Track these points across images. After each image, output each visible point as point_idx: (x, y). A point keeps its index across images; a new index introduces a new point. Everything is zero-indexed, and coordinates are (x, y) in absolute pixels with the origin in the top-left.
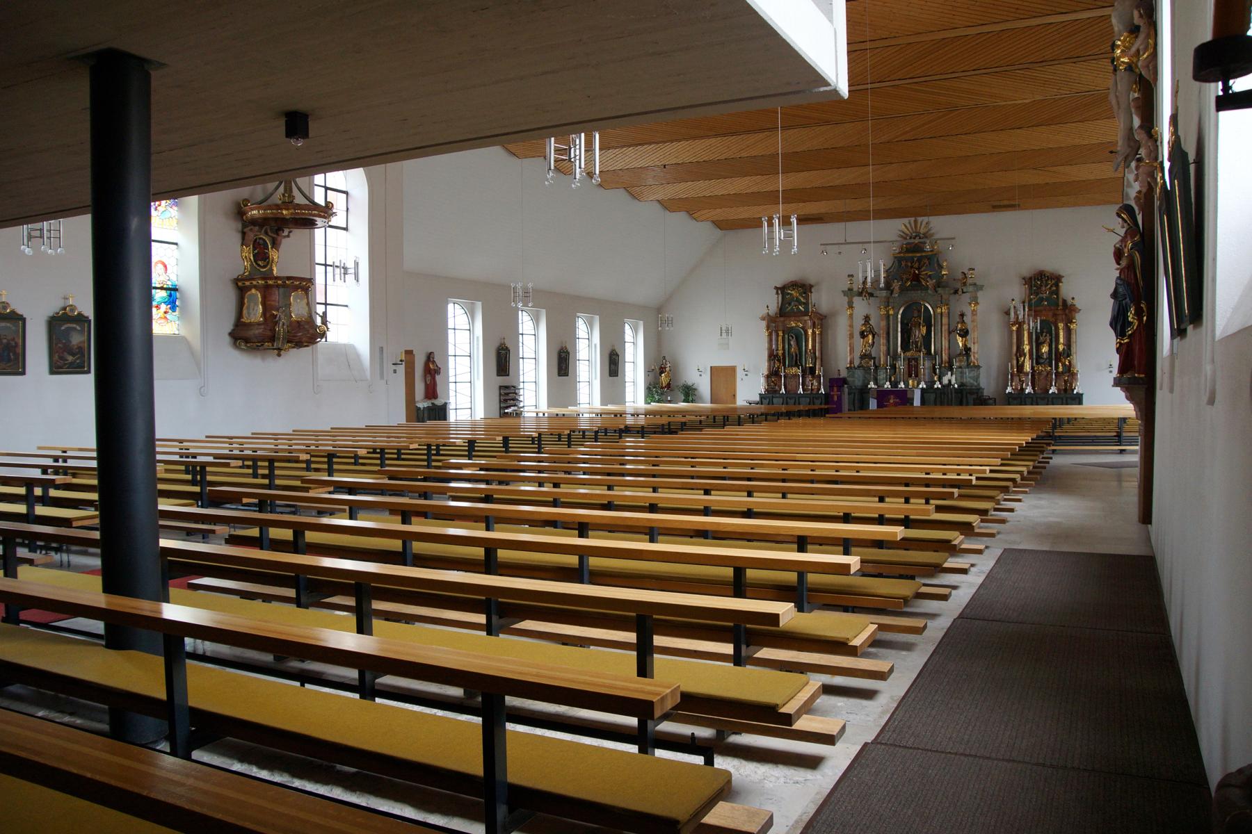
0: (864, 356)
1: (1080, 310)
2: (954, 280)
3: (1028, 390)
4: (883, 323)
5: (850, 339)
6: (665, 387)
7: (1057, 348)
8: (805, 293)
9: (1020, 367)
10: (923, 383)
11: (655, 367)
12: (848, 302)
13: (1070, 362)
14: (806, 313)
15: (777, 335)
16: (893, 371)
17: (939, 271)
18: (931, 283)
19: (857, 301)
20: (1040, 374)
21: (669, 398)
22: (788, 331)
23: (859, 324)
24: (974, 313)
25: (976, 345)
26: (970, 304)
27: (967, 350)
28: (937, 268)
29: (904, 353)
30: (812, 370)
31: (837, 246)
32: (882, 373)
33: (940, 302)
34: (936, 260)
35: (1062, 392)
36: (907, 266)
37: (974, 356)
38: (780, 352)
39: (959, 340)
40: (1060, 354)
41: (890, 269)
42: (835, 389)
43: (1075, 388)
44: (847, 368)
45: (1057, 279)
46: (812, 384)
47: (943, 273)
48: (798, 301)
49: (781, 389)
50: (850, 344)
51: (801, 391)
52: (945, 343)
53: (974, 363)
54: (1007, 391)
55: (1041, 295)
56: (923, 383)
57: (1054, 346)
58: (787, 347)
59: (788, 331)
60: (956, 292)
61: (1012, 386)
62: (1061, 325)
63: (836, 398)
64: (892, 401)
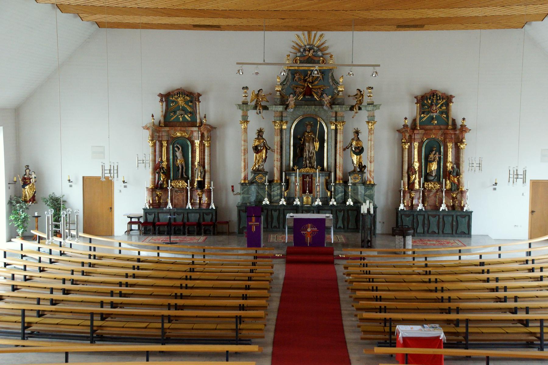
0: (256, 172)
1: (470, 130)
2: (349, 96)
3: (420, 207)
4: (277, 139)
5: (245, 154)
6: (30, 201)
7: (445, 167)
8: (191, 102)
9: (411, 185)
10: (318, 200)
11: (17, 178)
12: (243, 116)
13: (458, 180)
14: (193, 124)
15: (161, 146)
17: (334, 87)
18: (327, 99)
19: (252, 114)
20: (430, 191)
21: (36, 214)
22: (173, 141)
23: (252, 141)
24: (372, 132)
25: (372, 164)
26: (368, 122)
27: (362, 168)
28: (331, 84)
30: (201, 184)
31: (256, 66)
32: (276, 188)
34: (330, 75)
35: (450, 209)
37: (370, 175)
38: (165, 164)
39: (355, 158)
40: (450, 173)
42: (254, 219)
43: (464, 206)
44: (242, 184)
45: (448, 99)
46: (200, 199)
47: (340, 89)
48: (184, 109)
49: (166, 204)
50: (245, 159)
51: (189, 206)
52: (340, 160)
53: (370, 181)
54: (400, 208)
55: (432, 114)
56: (318, 200)
57: (442, 164)
58: (171, 157)
59: (173, 141)
60: (352, 108)
61: (404, 203)
62: (450, 145)
63: (254, 229)
64: (309, 230)
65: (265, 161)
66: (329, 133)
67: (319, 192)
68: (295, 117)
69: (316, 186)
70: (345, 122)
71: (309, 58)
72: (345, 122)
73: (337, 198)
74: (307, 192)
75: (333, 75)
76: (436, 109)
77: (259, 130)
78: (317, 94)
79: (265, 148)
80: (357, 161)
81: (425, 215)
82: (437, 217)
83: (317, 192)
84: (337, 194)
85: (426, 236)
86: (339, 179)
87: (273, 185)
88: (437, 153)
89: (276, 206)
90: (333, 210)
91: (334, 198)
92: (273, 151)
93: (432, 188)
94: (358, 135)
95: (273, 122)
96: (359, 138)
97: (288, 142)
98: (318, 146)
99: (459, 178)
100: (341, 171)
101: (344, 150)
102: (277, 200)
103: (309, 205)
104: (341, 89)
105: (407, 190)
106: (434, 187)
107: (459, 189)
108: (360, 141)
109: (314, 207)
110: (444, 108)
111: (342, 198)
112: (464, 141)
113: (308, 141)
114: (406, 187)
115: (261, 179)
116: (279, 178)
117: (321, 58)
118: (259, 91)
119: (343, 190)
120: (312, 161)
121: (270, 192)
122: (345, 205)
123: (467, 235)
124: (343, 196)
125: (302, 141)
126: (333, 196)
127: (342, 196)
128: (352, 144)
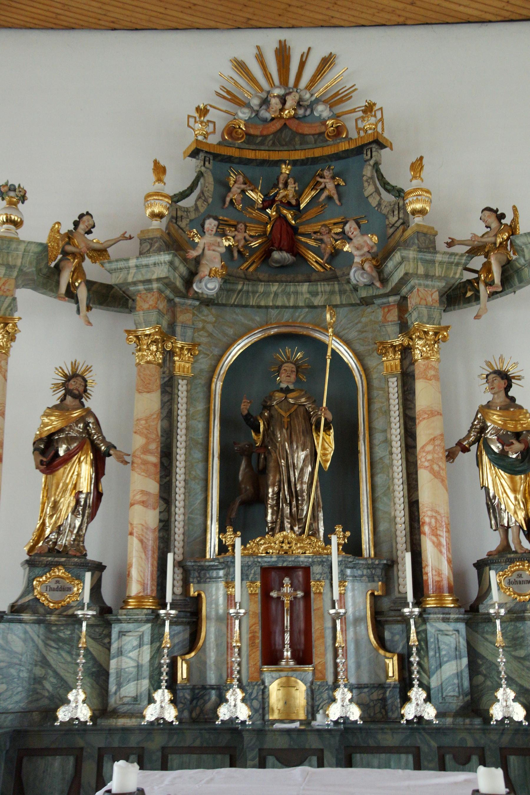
16: (184, 634)
29: (244, 543)
32: (130, 641)
33: (392, 329)
36: (250, 203)
41: (184, 195)
65: (92, 516)
66: (375, 393)
67: (345, 656)
68: (231, 332)
69: (329, 624)
70: (446, 328)
71: (281, 130)
72: (446, 328)
73: (434, 683)
74: (287, 654)
75: (378, 171)
77: (68, 371)
78: (317, 251)
79: (87, 447)
80: (516, 499)
83: (336, 656)
84: (433, 663)
86: (439, 590)
87: (119, 621)
89: (125, 730)
90: (424, 749)
91: (421, 685)
92: (127, 459)
94: (509, 387)
95: (129, 332)
96: (513, 399)
97: (200, 437)
98: (331, 451)
100: (444, 550)
101: (451, 455)
102: (136, 699)
103: (297, 725)
104: (418, 206)
108: (521, 408)
109: (320, 732)
111: (460, 686)
113: (286, 420)
115: (58, 594)
116: (151, 589)
117: (329, 122)
118: (76, 224)
119: (463, 643)
120: (307, 510)
121: (101, 659)
122: (478, 721)
124: (466, 674)
125: (257, 431)
126: (415, 675)
127: (459, 675)
128: (483, 429)
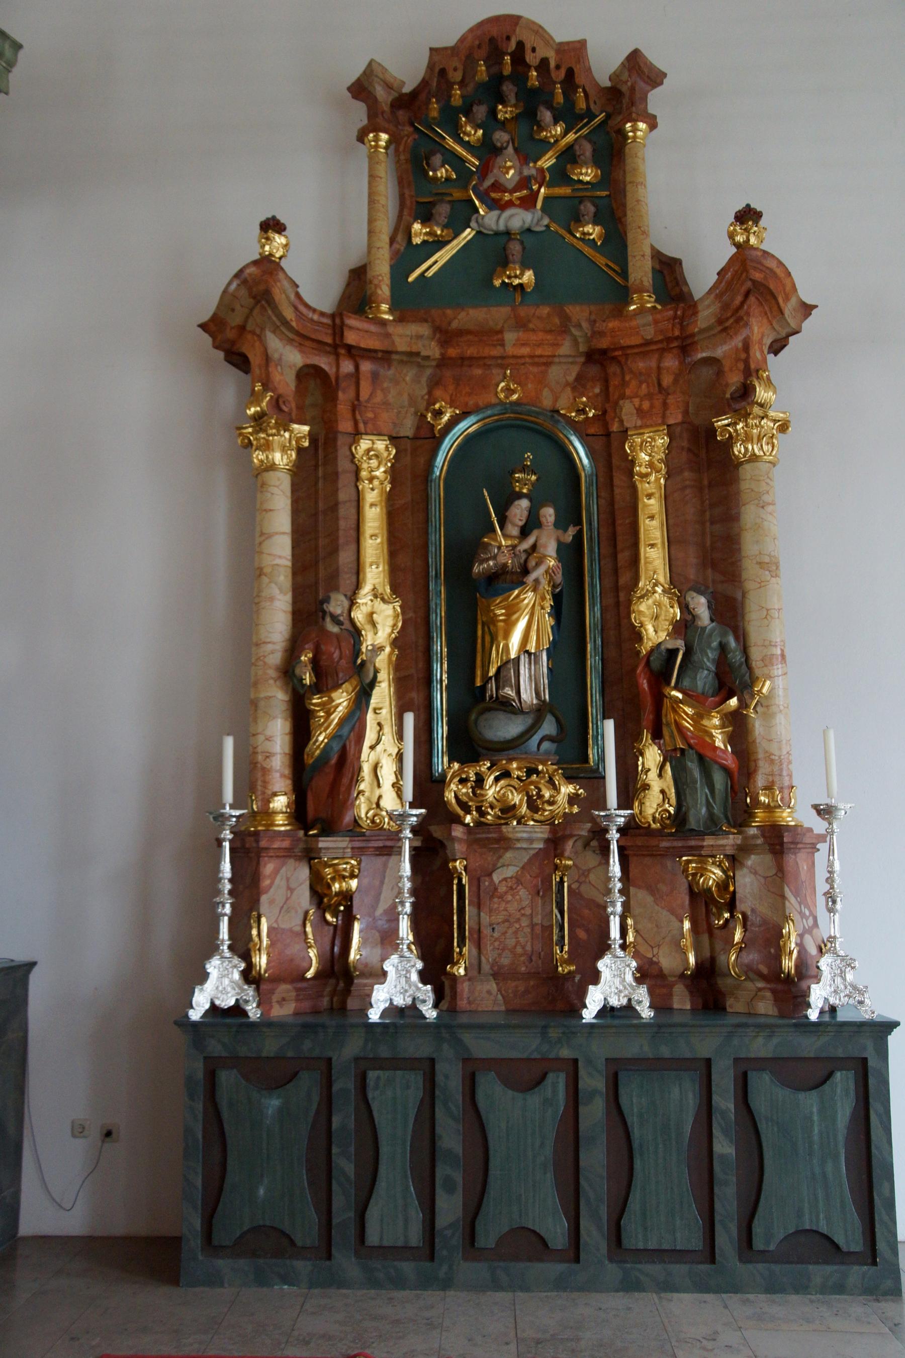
35: (681, 1000)
57: (592, 615)
76: (524, 182)
81: (441, 1068)
82: (557, 1083)
85: (446, 1284)
88: (548, 514)
93: (508, 810)
99: (743, 704)
105: (281, 823)
106: (533, 806)
107: (748, 814)
110: (587, 174)
112: (762, 394)
114: (280, 802)
123: (856, 1273)
